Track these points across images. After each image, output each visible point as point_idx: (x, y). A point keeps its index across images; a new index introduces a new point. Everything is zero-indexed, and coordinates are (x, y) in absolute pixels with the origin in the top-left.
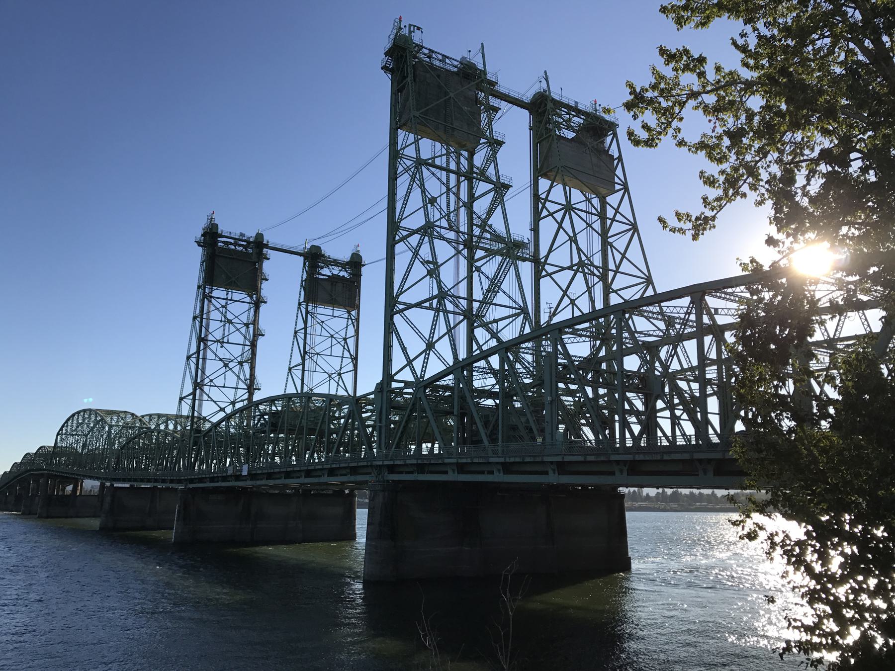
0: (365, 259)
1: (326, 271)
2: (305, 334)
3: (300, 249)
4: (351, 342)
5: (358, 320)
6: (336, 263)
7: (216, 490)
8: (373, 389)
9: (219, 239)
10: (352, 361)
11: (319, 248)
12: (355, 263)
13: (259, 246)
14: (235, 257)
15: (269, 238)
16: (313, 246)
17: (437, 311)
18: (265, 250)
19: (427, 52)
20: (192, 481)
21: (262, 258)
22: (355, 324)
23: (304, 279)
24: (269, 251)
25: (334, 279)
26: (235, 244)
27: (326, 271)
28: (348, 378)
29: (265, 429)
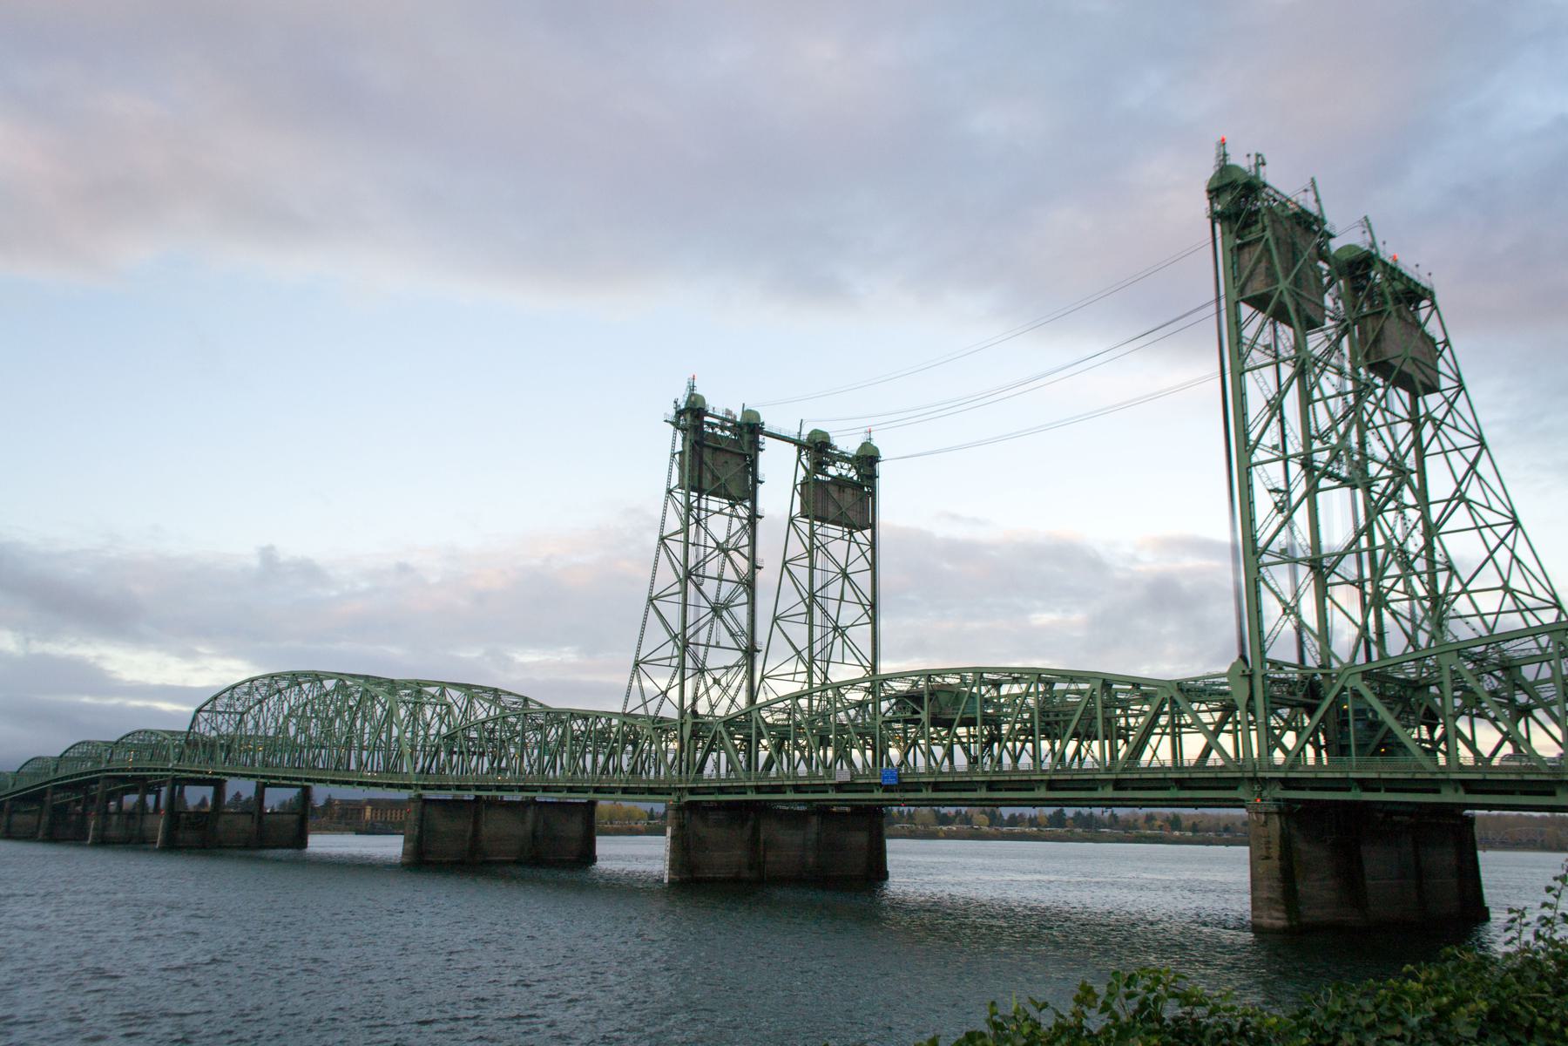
0: (883, 454)
1: (832, 471)
2: (812, 567)
3: (793, 435)
4: (863, 581)
5: (873, 545)
6: (842, 457)
7: (720, 806)
8: (1225, 669)
9: (707, 419)
10: (866, 612)
11: (825, 435)
12: (867, 460)
13: (750, 431)
14: (723, 446)
15: (770, 421)
16: (815, 432)
17: (731, 516)
18: (761, 437)
19: (1271, 192)
20: (692, 791)
21: (756, 448)
22: (868, 555)
23: (798, 481)
24: (767, 439)
25: (840, 482)
26: (723, 428)
27: (832, 471)
28: (861, 636)
29: (916, 716)
